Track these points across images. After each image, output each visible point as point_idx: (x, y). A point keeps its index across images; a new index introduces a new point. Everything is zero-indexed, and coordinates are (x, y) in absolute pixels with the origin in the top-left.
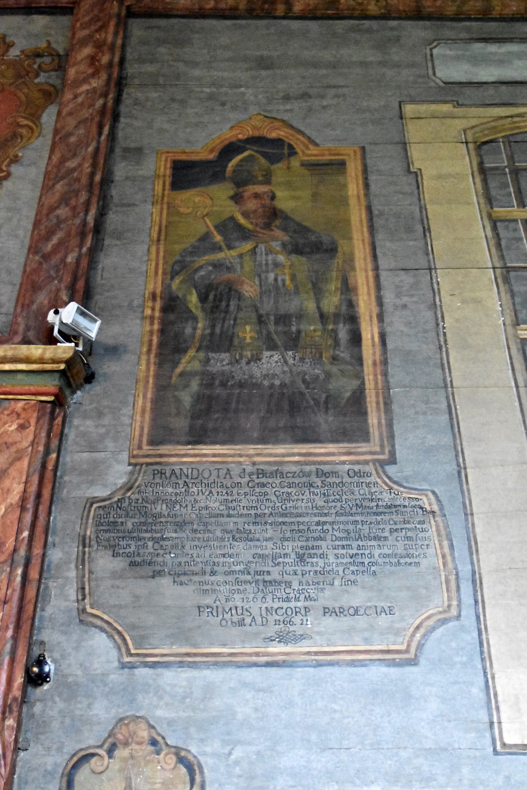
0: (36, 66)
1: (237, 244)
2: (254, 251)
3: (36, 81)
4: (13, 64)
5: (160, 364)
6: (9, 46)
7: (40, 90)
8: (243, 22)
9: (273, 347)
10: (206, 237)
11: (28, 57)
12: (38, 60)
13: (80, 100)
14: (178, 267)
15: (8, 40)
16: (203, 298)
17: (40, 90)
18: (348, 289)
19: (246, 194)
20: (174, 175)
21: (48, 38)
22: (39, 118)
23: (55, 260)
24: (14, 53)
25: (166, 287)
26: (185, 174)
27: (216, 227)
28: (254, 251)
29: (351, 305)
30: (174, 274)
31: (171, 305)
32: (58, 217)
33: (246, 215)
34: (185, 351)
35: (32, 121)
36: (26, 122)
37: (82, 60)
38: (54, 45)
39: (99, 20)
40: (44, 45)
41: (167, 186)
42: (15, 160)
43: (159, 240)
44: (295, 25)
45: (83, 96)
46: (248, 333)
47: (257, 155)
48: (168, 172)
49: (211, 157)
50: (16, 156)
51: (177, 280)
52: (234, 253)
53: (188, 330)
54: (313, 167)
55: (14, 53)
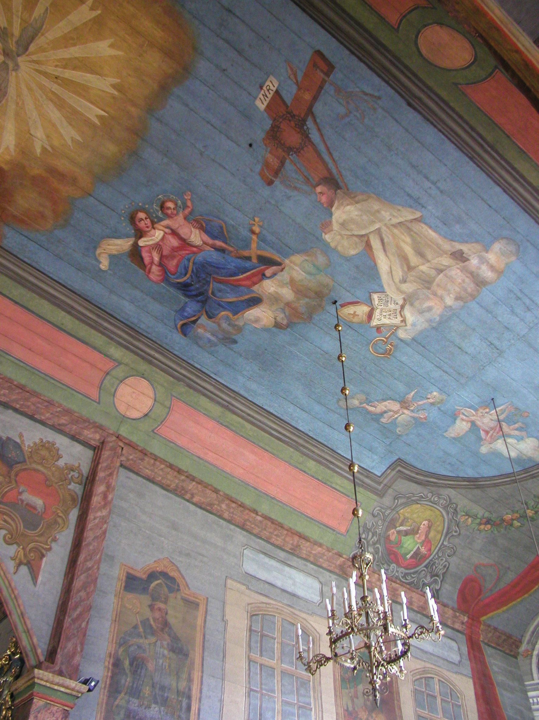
0: (70, 476)
1: (149, 637)
2: (155, 643)
3: (69, 487)
4: (58, 468)
5: (109, 697)
6: (60, 457)
7: (70, 494)
8: (170, 495)
9: (156, 703)
10: (135, 627)
11: (67, 468)
12: (72, 473)
13: (97, 521)
14: (122, 642)
15: (60, 452)
16: (131, 664)
17: (70, 494)
18: (190, 680)
19: (156, 607)
20: (126, 582)
21: (80, 461)
22: (68, 514)
23: (77, 625)
24: (61, 463)
25: (116, 652)
26: (132, 583)
27: (141, 622)
28: (155, 643)
29: (190, 689)
30: (120, 645)
31: (117, 664)
32: (81, 597)
33: (155, 620)
34: (120, 692)
35: (65, 515)
36: (60, 514)
37: (100, 493)
38: (81, 467)
39: (110, 469)
40: (77, 465)
41: (122, 588)
42: (55, 540)
43: (115, 621)
44: (192, 508)
45: (98, 519)
46: (147, 691)
47: (164, 585)
48: (124, 578)
49: (144, 577)
50: (55, 537)
51: (121, 649)
52: (147, 642)
53: (123, 681)
54: (186, 601)
55: (61, 463)
